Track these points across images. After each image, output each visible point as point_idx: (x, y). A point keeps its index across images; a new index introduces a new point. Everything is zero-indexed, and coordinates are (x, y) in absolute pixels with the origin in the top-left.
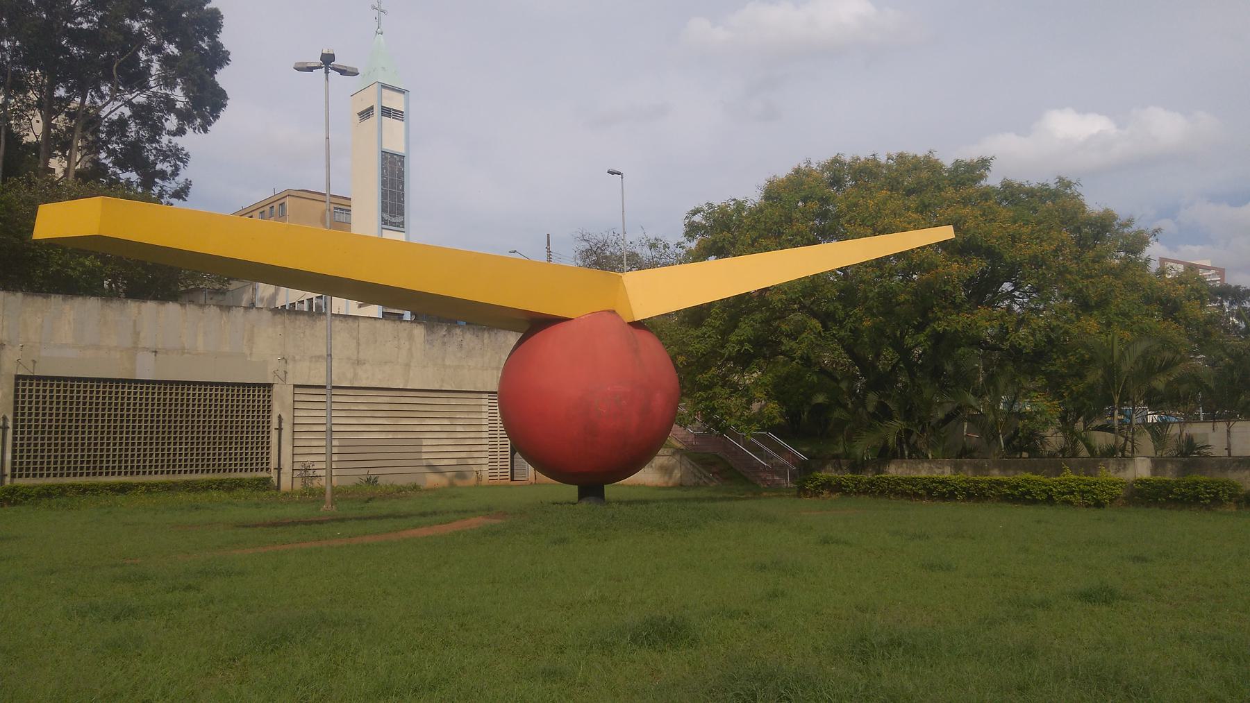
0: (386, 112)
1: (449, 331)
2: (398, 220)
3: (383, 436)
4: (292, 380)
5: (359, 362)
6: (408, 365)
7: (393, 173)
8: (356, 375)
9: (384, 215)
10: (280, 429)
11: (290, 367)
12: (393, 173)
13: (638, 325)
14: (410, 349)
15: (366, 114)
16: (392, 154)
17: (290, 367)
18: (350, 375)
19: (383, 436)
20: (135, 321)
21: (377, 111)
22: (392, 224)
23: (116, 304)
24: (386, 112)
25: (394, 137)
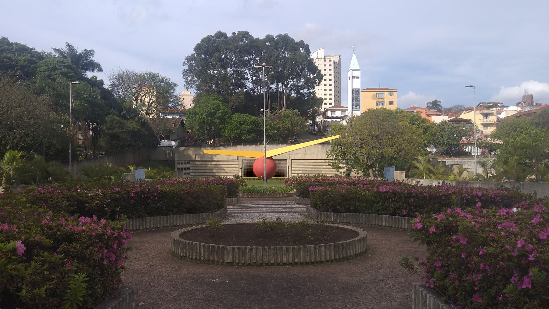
0: (353, 77)
1: (328, 146)
2: (358, 107)
3: (312, 170)
4: (291, 159)
5: (305, 154)
6: (317, 154)
7: (356, 94)
8: (305, 157)
9: (353, 107)
10: (289, 168)
11: (290, 156)
12: (356, 94)
13: (266, 158)
14: (318, 150)
15: (350, 78)
16: (356, 89)
17: (290, 156)
18: (304, 157)
19: (312, 170)
20: (261, 149)
21: (351, 78)
22: (355, 109)
23: (258, 146)
24: (353, 77)
25: (357, 84)
